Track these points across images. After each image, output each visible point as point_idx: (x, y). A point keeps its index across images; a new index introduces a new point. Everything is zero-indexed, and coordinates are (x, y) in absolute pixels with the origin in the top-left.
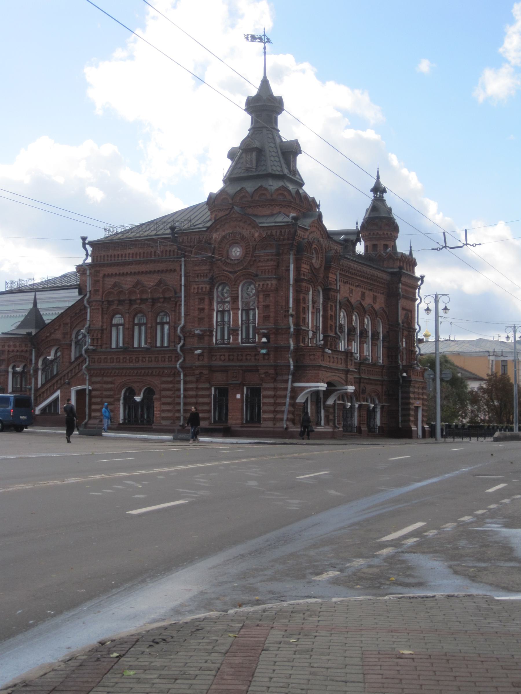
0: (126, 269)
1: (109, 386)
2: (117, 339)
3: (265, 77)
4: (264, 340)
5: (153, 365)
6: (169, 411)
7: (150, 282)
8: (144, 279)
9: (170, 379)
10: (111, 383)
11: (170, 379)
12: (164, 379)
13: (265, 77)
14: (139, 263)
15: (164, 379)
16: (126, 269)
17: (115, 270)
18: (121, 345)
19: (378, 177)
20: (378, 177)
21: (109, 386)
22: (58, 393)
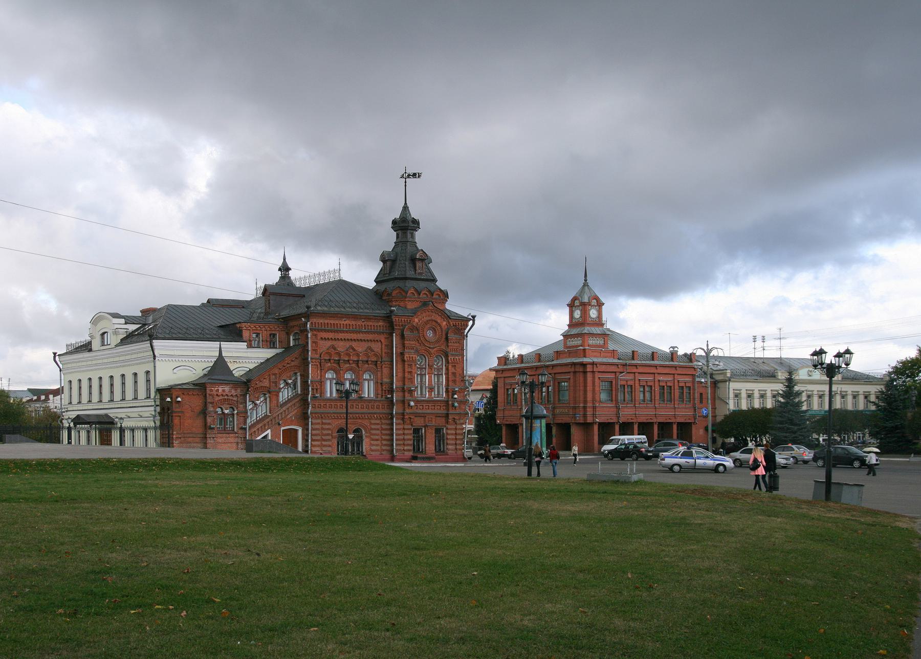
0: (341, 336)
1: (327, 427)
2: (330, 390)
3: (406, 203)
4: (456, 396)
5: (365, 410)
6: (377, 445)
7: (360, 348)
8: (354, 344)
9: (378, 422)
10: (329, 424)
11: (378, 422)
12: (373, 422)
13: (406, 203)
14: (353, 332)
15: (373, 422)
16: (360, 336)
17: (331, 335)
18: (334, 394)
19: (284, 259)
20: (284, 259)
21: (327, 427)
22: (269, 431)
